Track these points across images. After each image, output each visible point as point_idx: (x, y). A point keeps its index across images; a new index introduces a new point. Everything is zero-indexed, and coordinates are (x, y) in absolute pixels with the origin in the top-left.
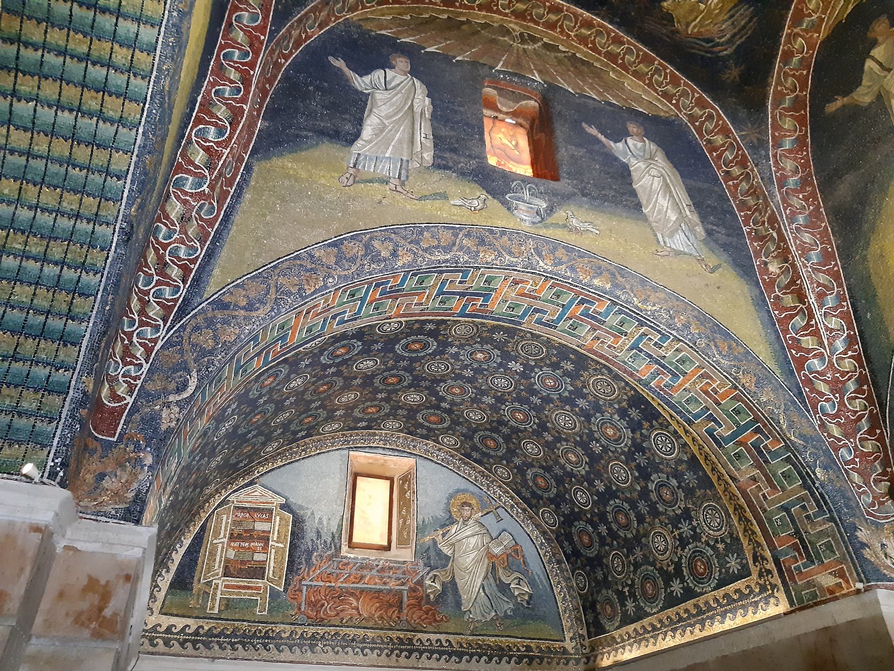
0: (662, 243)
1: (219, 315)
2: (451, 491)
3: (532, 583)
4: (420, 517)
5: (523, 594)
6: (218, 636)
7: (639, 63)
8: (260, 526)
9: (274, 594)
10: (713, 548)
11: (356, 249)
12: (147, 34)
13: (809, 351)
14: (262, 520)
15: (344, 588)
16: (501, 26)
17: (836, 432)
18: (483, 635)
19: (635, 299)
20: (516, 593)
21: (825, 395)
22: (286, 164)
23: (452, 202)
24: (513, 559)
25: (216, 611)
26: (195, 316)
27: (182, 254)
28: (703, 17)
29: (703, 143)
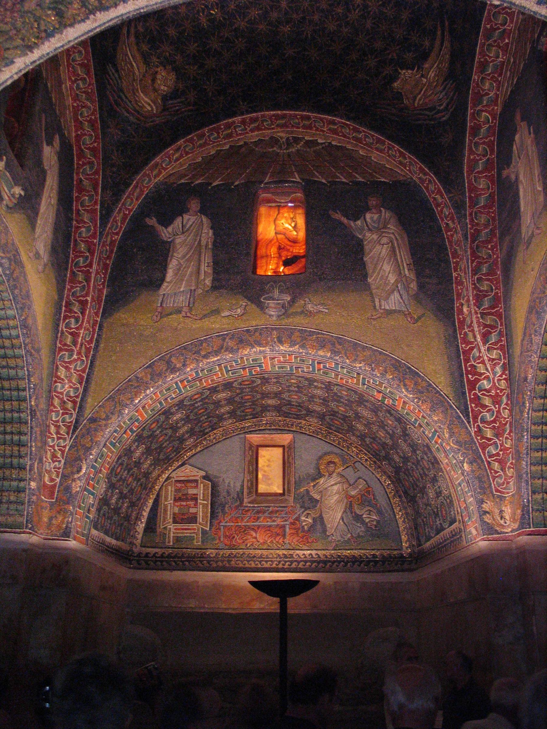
0: (377, 307)
1: (92, 426)
2: (320, 454)
3: (380, 513)
4: (297, 475)
5: (372, 521)
6: (174, 557)
7: (377, 143)
8: (191, 491)
9: (204, 532)
10: (446, 500)
11: (163, 366)
12: (14, 333)
13: (481, 374)
14: (192, 487)
15: (247, 525)
16: (272, 138)
17: (489, 434)
18: (341, 549)
19: (348, 361)
20: (367, 520)
21: (487, 406)
22: (123, 316)
23: (223, 315)
24: (366, 498)
25: (171, 544)
26: (81, 429)
27: (72, 394)
28: (426, 90)
29: (431, 200)
